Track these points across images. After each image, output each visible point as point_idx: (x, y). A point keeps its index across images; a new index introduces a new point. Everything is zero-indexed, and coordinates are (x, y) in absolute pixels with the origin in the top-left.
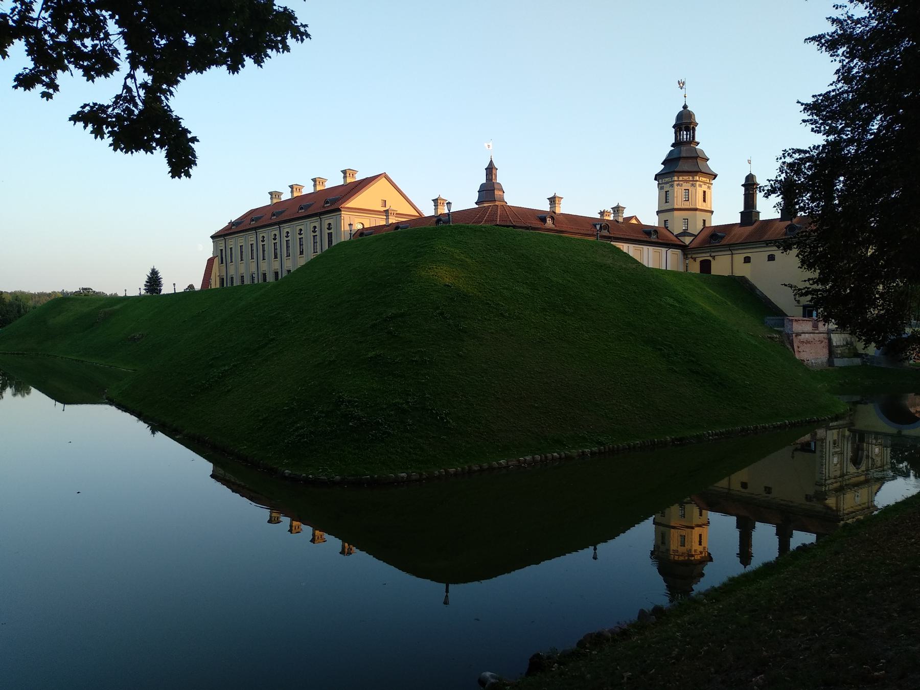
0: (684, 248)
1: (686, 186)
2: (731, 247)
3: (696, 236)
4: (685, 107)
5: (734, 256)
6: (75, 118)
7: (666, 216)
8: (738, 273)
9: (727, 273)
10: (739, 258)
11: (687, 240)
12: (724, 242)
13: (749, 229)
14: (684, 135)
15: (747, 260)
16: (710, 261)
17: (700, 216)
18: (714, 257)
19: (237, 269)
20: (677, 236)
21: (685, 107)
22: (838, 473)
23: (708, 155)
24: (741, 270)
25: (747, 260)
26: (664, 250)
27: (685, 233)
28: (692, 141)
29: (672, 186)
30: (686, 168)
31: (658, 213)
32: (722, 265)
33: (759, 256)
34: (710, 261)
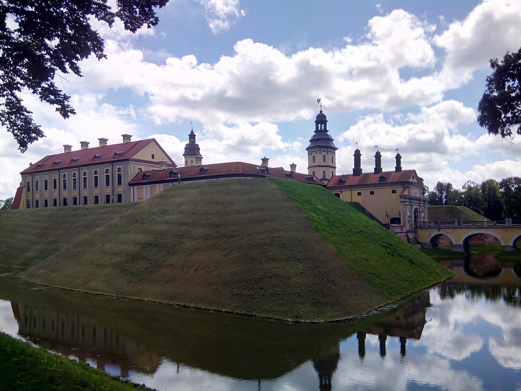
1: (324, 153)
2: (351, 187)
4: (321, 112)
5: (352, 192)
9: (350, 201)
10: (355, 193)
11: (326, 183)
12: (346, 184)
13: (358, 178)
14: (321, 127)
15: (359, 194)
17: (331, 170)
20: (320, 180)
21: (321, 112)
24: (357, 199)
25: (359, 194)
27: (324, 179)
28: (326, 131)
29: (317, 153)
32: (346, 196)
33: (366, 192)
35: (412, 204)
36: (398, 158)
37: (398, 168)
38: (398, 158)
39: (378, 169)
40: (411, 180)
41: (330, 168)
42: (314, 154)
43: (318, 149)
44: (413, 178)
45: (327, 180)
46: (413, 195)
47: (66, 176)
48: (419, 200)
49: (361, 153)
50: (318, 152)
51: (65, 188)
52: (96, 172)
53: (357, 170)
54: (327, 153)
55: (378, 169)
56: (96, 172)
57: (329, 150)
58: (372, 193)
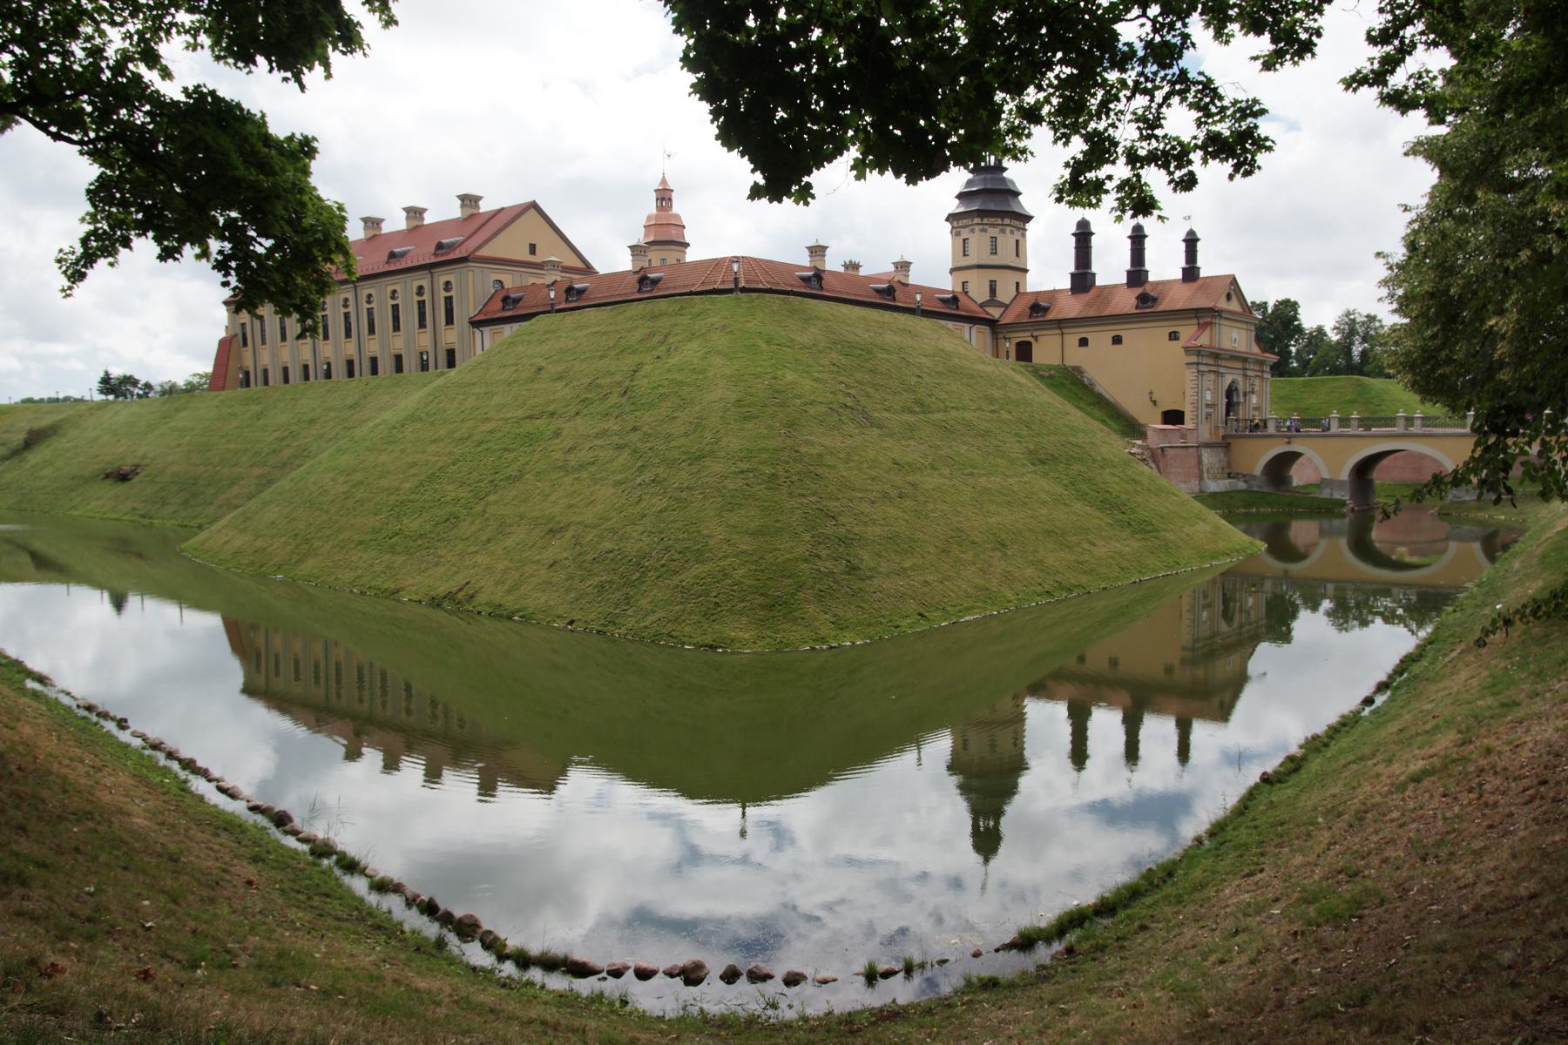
0: (992, 323)
1: (994, 232)
2: (1062, 324)
3: (1007, 306)
6: (1406, 154)
7: (964, 276)
8: (1069, 362)
9: (1056, 361)
10: (1072, 339)
11: (995, 313)
12: (1050, 316)
15: (1083, 342)
16: (1029, 344)
17: (1012, 277)
18: (1036, 338)
19: (274, 355)
20: (981, 306)
22: (1208, 633)
23: (1020, 187)
24: (1076, 357)
26: (967, 326)
27: (993, 301)
30: (992, 207)
31: (952, 271)
33: (1100, 338)
34: (1029, 344)
35: (1221, 370)
36: (1191, 242)
37: (1191, 273)
38: (1191, 242)
39: (1137, 275)
40: (1222, 304)
41: (1008, 272)
42: (965, 233)
43: (977, 220)
44: (1229, 297)
45: (1000, 305)
46: (1226, 345)
47: (374, 299)
48: (1245, 360)
49: (1093, 229)
50: (977, 228)
51: (372, 330)
52: (420, 290)
53: (1082, 278)
54: (1003, 231)
55: (1137, 275)
56: (420, 290)
57: (1007, 221)
58: (1117, 340)
